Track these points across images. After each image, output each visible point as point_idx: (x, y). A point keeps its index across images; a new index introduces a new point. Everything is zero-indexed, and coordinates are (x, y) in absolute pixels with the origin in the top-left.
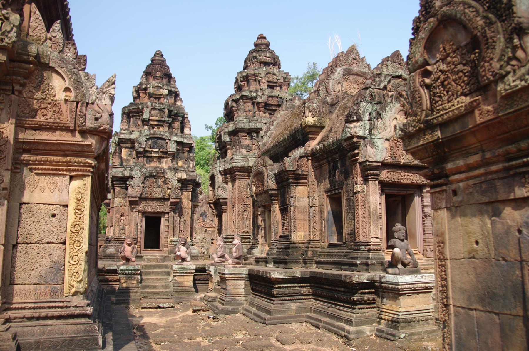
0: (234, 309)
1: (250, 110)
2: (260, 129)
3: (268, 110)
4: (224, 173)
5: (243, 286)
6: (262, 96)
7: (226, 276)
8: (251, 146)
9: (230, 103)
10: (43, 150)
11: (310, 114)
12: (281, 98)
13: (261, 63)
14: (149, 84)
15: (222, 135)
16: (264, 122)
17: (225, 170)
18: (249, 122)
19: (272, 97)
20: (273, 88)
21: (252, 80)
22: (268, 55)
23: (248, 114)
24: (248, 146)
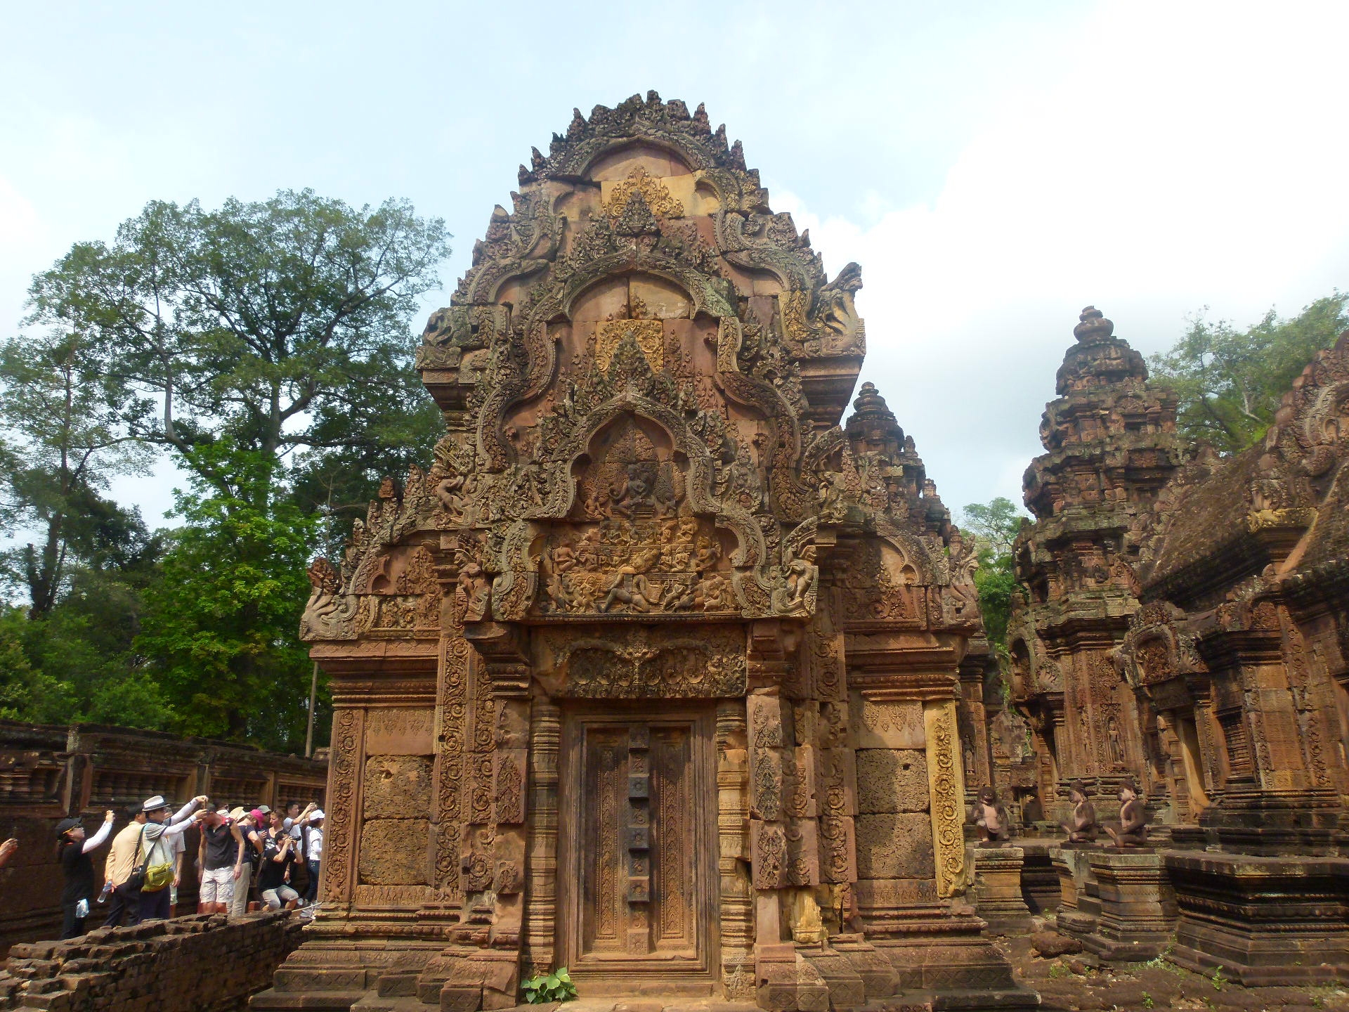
0: (1145, 949)
1: (1090, 488)
2: (1124, 529)
3: (1134, 481)
4: (1049, 635)
5: (1157, 897)
6: (1117, 454)
7: (1115, 872)
8: (1105, 568)
9: (1038, 476)
11: (1267, 503)
12: (1162, 450)
13: (1098, 374)
14: (861, 458)
15: (1032, 548)
16: (1132, 511)
17: (1050, 628)
18: (1093, 515)
19: (1141, 451)
20: (1138, 429)
21: (1085, 417)
22: (1113, 355)
23: (1088, 498)
24: (1097, 569)
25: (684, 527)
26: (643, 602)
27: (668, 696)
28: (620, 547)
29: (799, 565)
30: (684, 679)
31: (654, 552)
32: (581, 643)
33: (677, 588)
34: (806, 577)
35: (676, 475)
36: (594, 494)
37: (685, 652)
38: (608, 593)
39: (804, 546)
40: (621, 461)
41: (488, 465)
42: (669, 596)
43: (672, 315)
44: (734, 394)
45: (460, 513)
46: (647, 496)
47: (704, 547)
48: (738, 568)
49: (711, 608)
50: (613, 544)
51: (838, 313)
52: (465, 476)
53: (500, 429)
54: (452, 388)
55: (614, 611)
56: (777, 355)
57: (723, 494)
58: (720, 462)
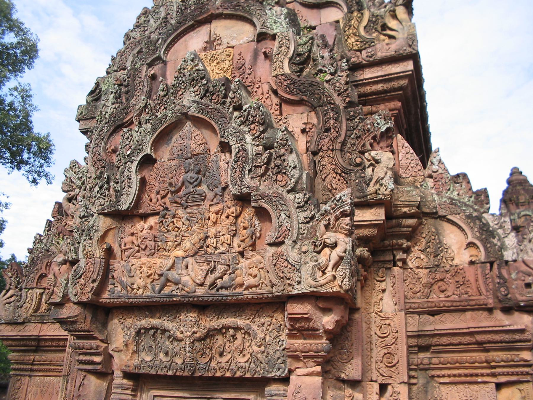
26: (190, 283)
28: (174, 234)
29: (331, 237)
31: (202, 235)
33: (221, 268)
34: (339, 250)
36: (156, 189)
38: (161, 275)
43: (241, 42)
46: (199, 185)
47: (245, 228)
48: (270, 245)
49: (251, 287)
55: (166, 291)
57: (262, 175)
58: (261, 147)
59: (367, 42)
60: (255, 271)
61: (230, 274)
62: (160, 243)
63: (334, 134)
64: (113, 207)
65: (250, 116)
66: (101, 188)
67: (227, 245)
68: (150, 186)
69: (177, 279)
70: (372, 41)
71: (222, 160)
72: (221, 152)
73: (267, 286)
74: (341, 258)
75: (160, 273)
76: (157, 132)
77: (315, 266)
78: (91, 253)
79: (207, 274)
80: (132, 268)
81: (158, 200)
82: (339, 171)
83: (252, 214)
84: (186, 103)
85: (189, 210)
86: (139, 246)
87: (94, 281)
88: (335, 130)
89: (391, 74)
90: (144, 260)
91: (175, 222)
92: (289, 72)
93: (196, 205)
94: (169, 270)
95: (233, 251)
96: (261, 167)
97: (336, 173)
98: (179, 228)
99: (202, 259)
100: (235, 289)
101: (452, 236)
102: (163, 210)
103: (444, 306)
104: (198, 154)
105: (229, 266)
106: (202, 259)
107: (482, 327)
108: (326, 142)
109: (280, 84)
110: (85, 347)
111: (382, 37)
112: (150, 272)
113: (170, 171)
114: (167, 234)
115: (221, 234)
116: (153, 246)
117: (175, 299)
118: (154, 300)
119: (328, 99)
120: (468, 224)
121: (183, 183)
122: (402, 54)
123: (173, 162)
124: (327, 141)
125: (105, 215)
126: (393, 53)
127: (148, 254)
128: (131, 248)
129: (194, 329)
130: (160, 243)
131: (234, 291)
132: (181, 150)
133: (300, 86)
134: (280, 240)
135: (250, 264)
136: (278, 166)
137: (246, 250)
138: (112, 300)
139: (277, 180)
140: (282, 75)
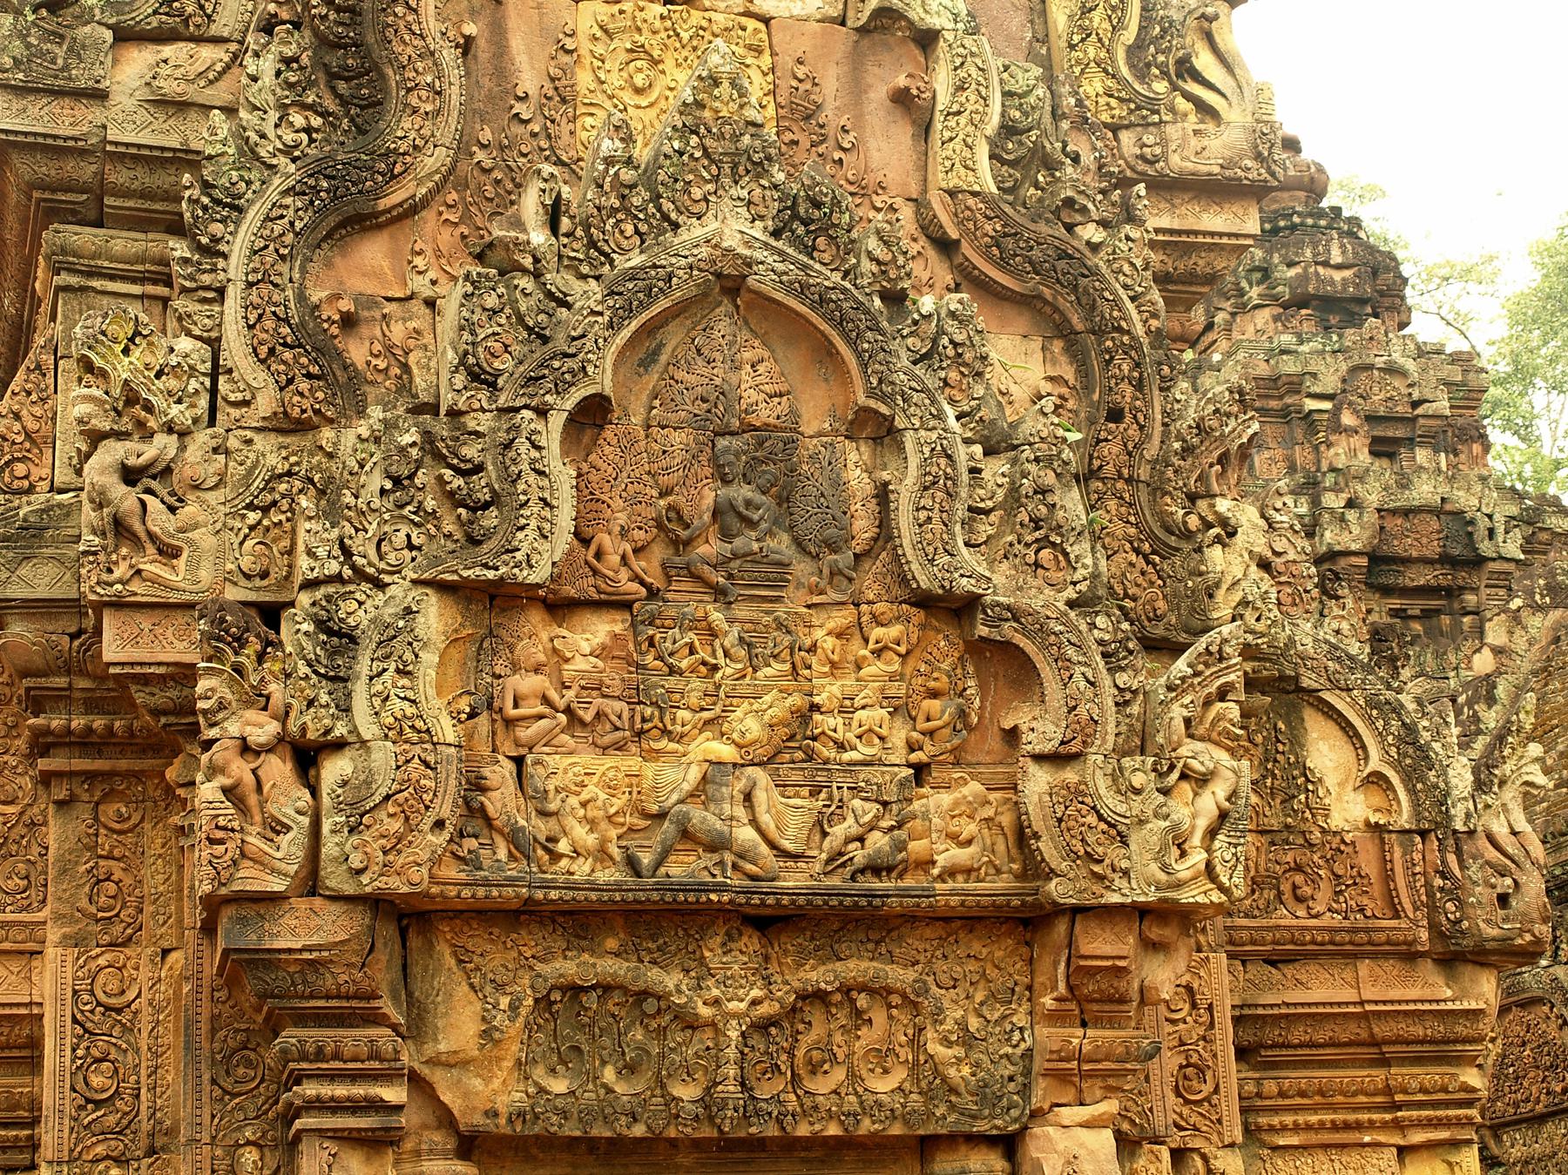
10: (1301, 1045)
25: (877, 632)
26: (764, 849)
27: (803, 1130)
29: (1200, 754)
30: (853, 1076)
31: (796, 700)
32: (567, 967)
34: (1219, 790)
35: (858, 480)
36: (622, 518)
37: (862, 1001)
38: (661, 816)
39: (1207, 703)
40: (699, 423)
41: (266, 404)
42: (839, 831)
44: (989, 258)
45: (169, 553)
47: (934, 694)
48: (1039, 758)
49: (951, 872)
50: (673, 671)
51: (1204, 61)
52: (183, 434)
53: (301, 297)
54: (83, 153)
56: (1088, 158)
59: (1138, 108)
60: (969, 829)
61: (891, 829)
62: (648, 711)
63: (1133, 431)
64: (486, 566)
65: (945, 341)
66: (397, 481)
67: (877, 741)
68: (593, 505)
69: (721, 833)
70: (1152, 104)
71: (850, 465)
72: (847, 437)
73: (998, 871)
74: (1223, 816)
75: (654, 809)
76: (634, 325)
77: (1168, 830)
78: (419, 724)
79: (819, 823)
80: (552, 787)
81: (624, 557)
82: (1146, 547)
83: (956, 654)
84: (731, 241)
85: (742, 611)
86: (568, 711)
87: (439, 824)
88: (1135, 417)
89: (1196, 233)
90: (587, 759)
91: (697, 643)
92: (994, 190)
93: (765, 599)
94: (681, 801)
95: (894, 759)
96: (987, 512)
97: (1137, 551)
98: (715, 668)
99: (796, 777)
100: (901, 876)
101: (1323, 746)
102: (647, 599)
103: (1314, 942)
104: (766, 427)
105: (885, 804)
106: (796, 777)
107: (1392, 1002)
108: (1111, 450)
109: (971, 225)
110: (347, 1051)
111: (1182, 104)
112: (618, 803)
113: (664, 464)
114: (671, 682)
115: (858, 702)
116: (626, 715)
117: (713, 897)
118: (642, 896)
119: (1115, 314)
120: (1371, 722)
121: (716, 513)
122: (1240, 179)
123: (678, 438)
124: (1115, 450)
125: (442, 587)
126: (1216, 170)
127: (608, 739)
128: (541, 717)
129: (756, 993)
130: (648, 711)
131: (900, 884)
132: (704, 400)
133: (1032, 248)
134: (1074, 748)
135: (956, 804)
136: (1036, 523)
137: (941, 763)
138: (481, 892)
139: (1037, 565)
140: (975, 194)
